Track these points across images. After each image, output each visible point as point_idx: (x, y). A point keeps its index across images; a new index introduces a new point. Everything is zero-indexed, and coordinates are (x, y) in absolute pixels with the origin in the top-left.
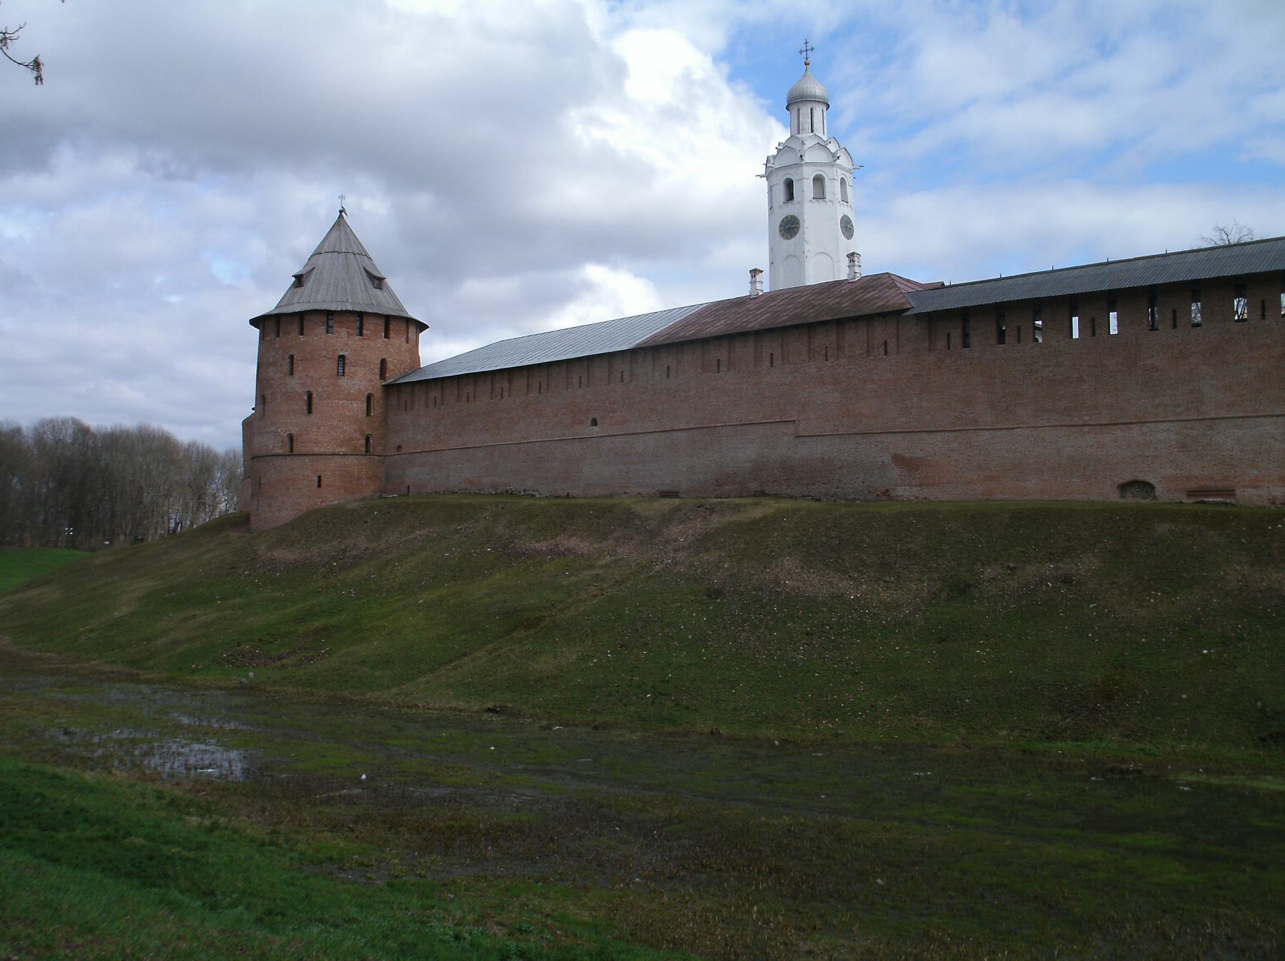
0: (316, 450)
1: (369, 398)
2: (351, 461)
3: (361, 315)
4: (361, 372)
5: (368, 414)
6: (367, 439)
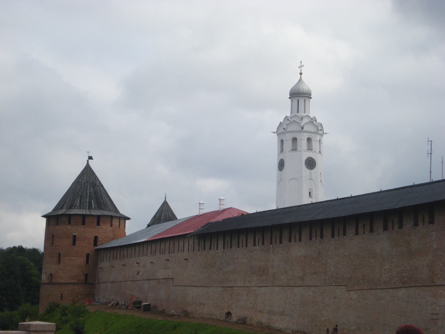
0: (61, 281)
1: (88, 255)
5: (87, 262)
6: (86, 275)
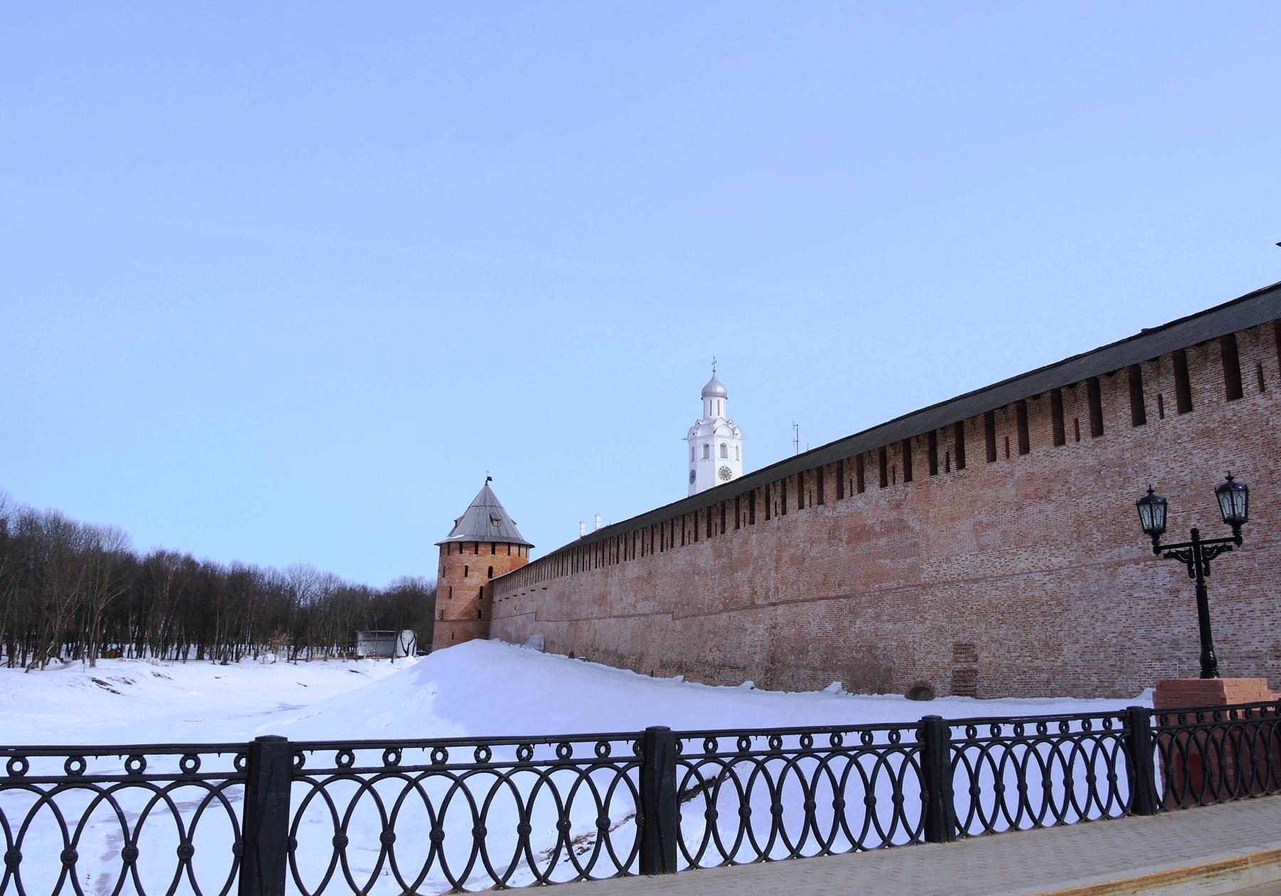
1: (482, 588)
2: (471, 624)
3: (476, 544)
4: (476, 574)
